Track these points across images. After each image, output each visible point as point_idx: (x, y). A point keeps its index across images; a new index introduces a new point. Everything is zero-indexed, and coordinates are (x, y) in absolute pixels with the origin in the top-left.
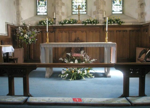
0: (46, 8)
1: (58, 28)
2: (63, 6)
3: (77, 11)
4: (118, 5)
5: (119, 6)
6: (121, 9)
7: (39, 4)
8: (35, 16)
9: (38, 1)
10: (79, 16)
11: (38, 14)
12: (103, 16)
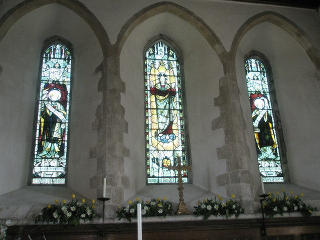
0: (65, 164)
2: (126, 159)
7: (41, 149)
8: (23, 187)
9: (37, 142)
11: (36, 181)
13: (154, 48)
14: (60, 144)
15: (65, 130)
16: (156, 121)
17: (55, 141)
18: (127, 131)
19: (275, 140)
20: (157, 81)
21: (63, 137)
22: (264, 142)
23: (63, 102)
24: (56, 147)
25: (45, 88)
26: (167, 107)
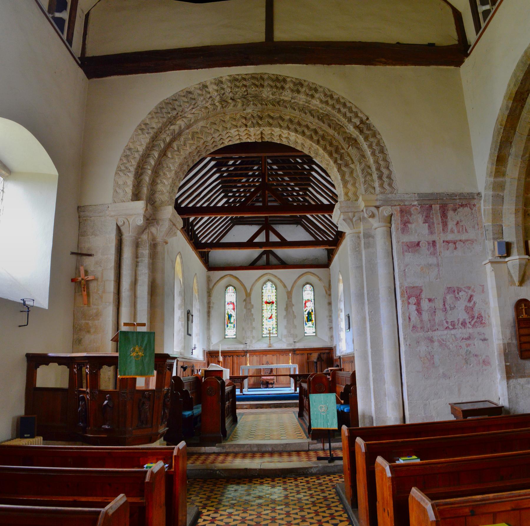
1: (249, 352)
2: (254, 330)
3: (268, 335)
4: (311, 327)
5: (311, 328)
6: (314, 331)
7: (227, 326)
10: (270, 339)
11: (226, 337)
13: (266, 284)
16: (266, 314)
17: (232, 323)
18: (254, 321)
19: (313, 319)
20: (267, 298)
21: (234, 322)
22: (309, 320)
23: (234, 309)
24: (232, 325)
25: (227, 304)
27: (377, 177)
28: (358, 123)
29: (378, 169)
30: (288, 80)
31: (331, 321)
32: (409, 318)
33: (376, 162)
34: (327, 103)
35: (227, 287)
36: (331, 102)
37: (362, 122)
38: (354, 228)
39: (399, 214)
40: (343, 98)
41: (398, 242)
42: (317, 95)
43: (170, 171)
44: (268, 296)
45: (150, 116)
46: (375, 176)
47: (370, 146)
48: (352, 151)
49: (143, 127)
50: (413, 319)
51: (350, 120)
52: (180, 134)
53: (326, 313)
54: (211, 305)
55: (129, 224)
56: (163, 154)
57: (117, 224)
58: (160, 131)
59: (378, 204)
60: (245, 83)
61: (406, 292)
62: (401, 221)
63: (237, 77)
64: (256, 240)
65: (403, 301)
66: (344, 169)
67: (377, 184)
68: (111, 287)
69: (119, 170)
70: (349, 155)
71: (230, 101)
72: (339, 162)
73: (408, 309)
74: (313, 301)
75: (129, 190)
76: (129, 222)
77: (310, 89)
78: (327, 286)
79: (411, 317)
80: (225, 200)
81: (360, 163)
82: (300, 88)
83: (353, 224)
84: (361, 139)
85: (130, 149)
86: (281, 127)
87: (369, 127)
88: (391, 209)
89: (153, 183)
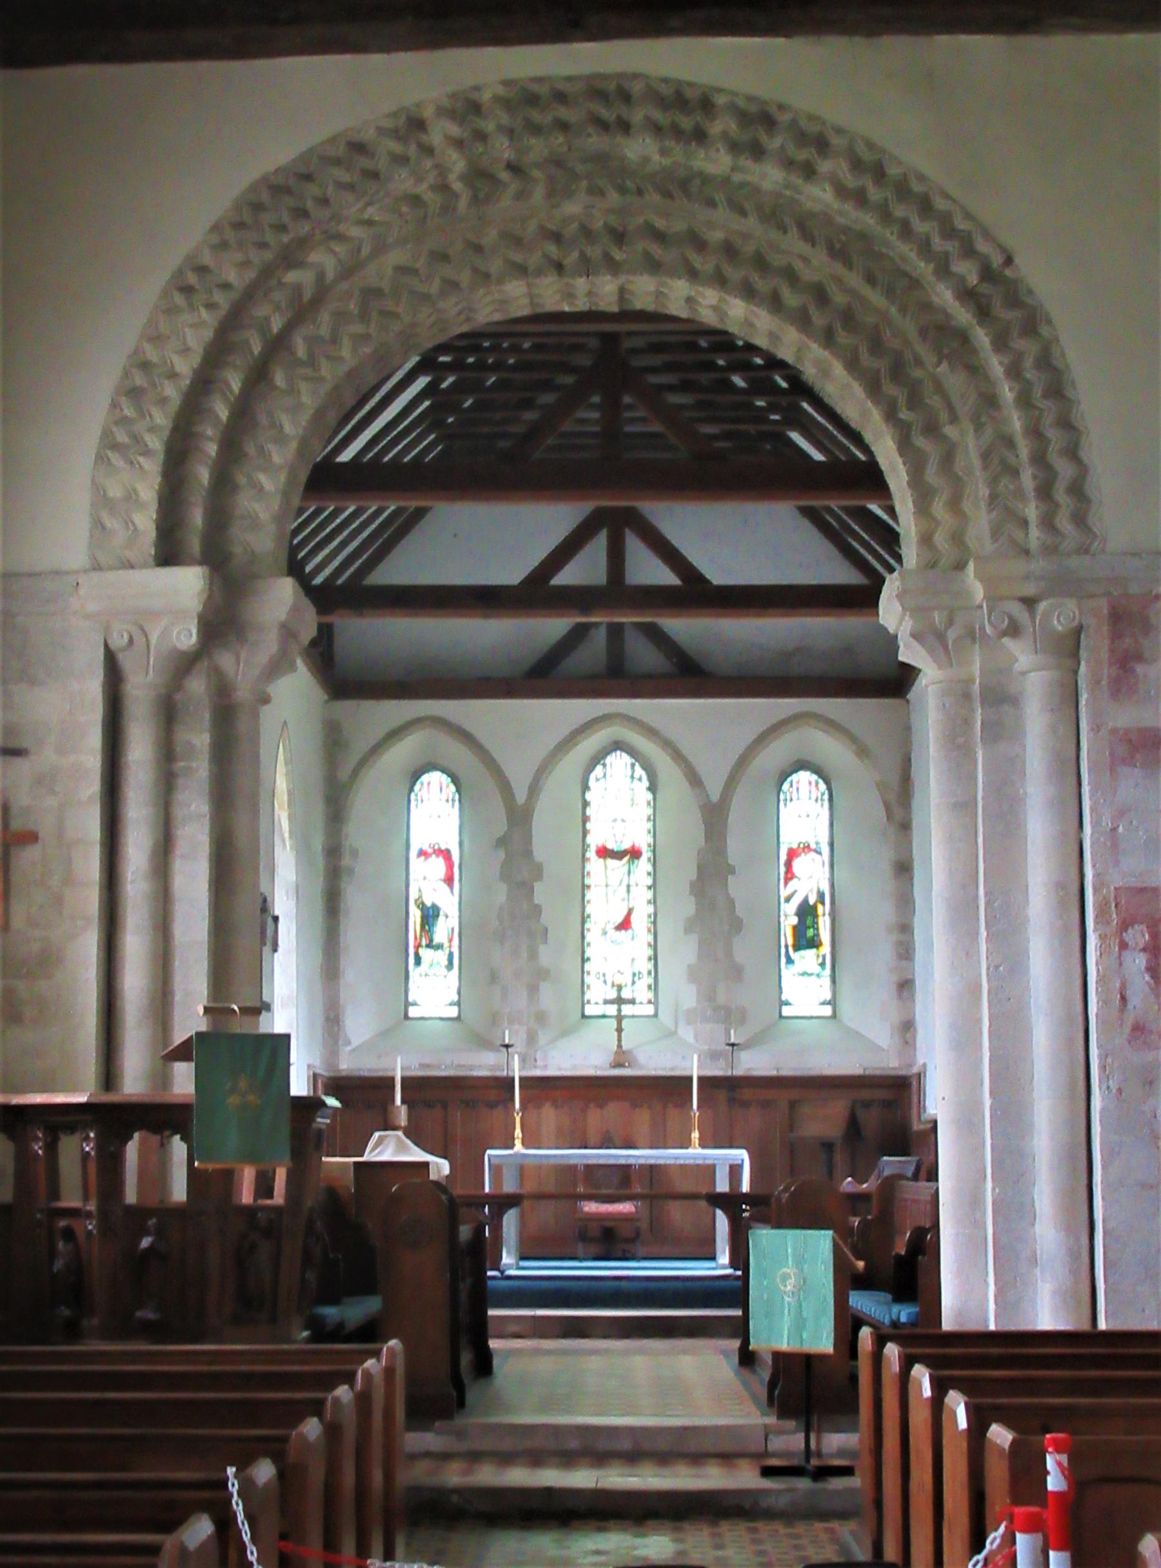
3: (612, 1010)
5: (814, 977)
7: (418, 961)
10: (619, 1030)
12: (729, 1036)
13: (604, 765)
14: (447, 952)
15: (453, 930)
17: (439, 947)
19: (825, 935)
21: (450, 941)
22: (804, 942)
23: (449, 880)
24: (441, 957)
26: (625, 883)
27: (1035, 490)
28: (973, 279)
29: (1040, 459)
30: (721, 100)
31: (907, 952)
32: (1123, 999)
33: (1035, 433)
34: (860, 198)
35: (416, 776)
36: (875, 194)
37: (987, 274)
38: (952, 666)
39: (1105, 629)
40: (922, 178)
41: (1096, 729)
42: (824, 166)
43: (281, 439)
44: (615, 820)
45: (215, 239)
46: (1028, 480)
47: (1014, 372)
48: (954, 381)
49: (192, 279)
50: (1134, 1001)
51: (943, 270)
52: (318, 300)
53: (887, 912)
54: (346, 861)
55: (148, 641)
56: (259, 376)
57: (106, 645)
58: (250, 295)
59: (1029, 590)
60: (563, 113)
61: (1116, 906)
62: (1112, 651)
63: (535, 88)
64: (566, 577)
65: (1102, 938)
66: (920, 442)
67: (1032, 511)
68: (91, 866)
69: (109, 443)
70: (939, 388)
71: (504, 176)
72: (904, 415)
73: (1121, 964)
74: (826, 850)
75: (146, 522)
76: (146, 636)
77: (801, 138)
78: (894, 780)
79: (1128, 993)
80: (422, 382)
81: (979, 428)
82: (764, 138)
83: (946, 648)
84: (982, 338)
85: (145, 366)
86: (693, 275)
87: (1015, 295)
88: (1079, 608)
89: (223, 484)
